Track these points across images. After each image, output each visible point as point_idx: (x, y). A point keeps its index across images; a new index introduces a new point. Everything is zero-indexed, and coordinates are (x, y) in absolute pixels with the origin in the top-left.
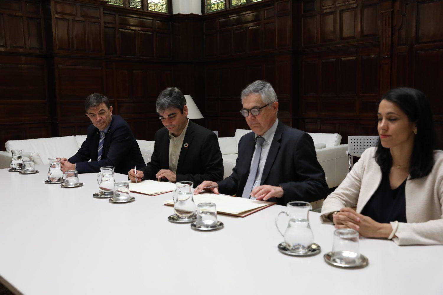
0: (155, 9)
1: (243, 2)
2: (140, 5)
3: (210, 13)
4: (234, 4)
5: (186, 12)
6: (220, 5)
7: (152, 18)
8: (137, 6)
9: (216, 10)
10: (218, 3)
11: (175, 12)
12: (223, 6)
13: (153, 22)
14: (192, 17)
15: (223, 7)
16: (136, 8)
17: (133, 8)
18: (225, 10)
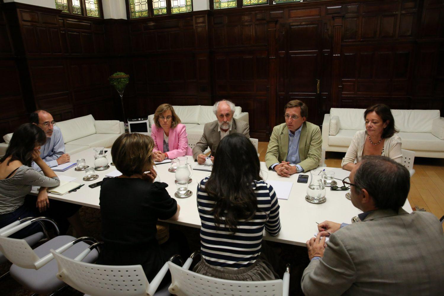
0: (91, 15)
1: (164, 12)
2: (80, 12)
3: (135, 18)
4: (156, 13)
5: (116, 17)
6: (144, 13)
7: (90, 22)
8: (78, 12)
9: (140, 17)
10: (142, 11)
11: (106, 17)
12: (146, 14)
13: (91, 24)
14: (120, 22)
15: (146, 15)
16: (78, 14)
17: (76, 14)
18: (149, 18)
